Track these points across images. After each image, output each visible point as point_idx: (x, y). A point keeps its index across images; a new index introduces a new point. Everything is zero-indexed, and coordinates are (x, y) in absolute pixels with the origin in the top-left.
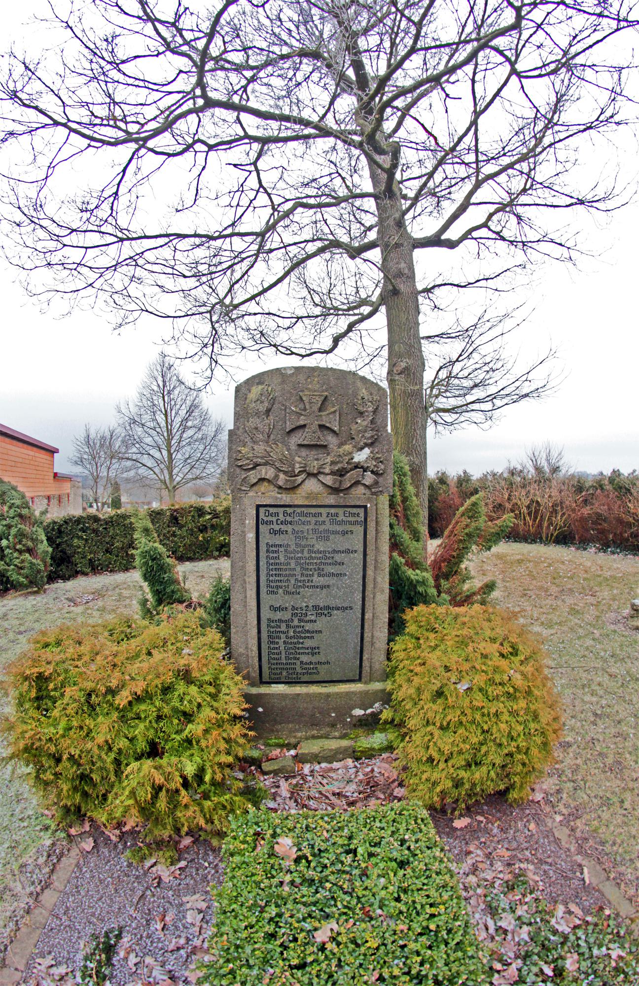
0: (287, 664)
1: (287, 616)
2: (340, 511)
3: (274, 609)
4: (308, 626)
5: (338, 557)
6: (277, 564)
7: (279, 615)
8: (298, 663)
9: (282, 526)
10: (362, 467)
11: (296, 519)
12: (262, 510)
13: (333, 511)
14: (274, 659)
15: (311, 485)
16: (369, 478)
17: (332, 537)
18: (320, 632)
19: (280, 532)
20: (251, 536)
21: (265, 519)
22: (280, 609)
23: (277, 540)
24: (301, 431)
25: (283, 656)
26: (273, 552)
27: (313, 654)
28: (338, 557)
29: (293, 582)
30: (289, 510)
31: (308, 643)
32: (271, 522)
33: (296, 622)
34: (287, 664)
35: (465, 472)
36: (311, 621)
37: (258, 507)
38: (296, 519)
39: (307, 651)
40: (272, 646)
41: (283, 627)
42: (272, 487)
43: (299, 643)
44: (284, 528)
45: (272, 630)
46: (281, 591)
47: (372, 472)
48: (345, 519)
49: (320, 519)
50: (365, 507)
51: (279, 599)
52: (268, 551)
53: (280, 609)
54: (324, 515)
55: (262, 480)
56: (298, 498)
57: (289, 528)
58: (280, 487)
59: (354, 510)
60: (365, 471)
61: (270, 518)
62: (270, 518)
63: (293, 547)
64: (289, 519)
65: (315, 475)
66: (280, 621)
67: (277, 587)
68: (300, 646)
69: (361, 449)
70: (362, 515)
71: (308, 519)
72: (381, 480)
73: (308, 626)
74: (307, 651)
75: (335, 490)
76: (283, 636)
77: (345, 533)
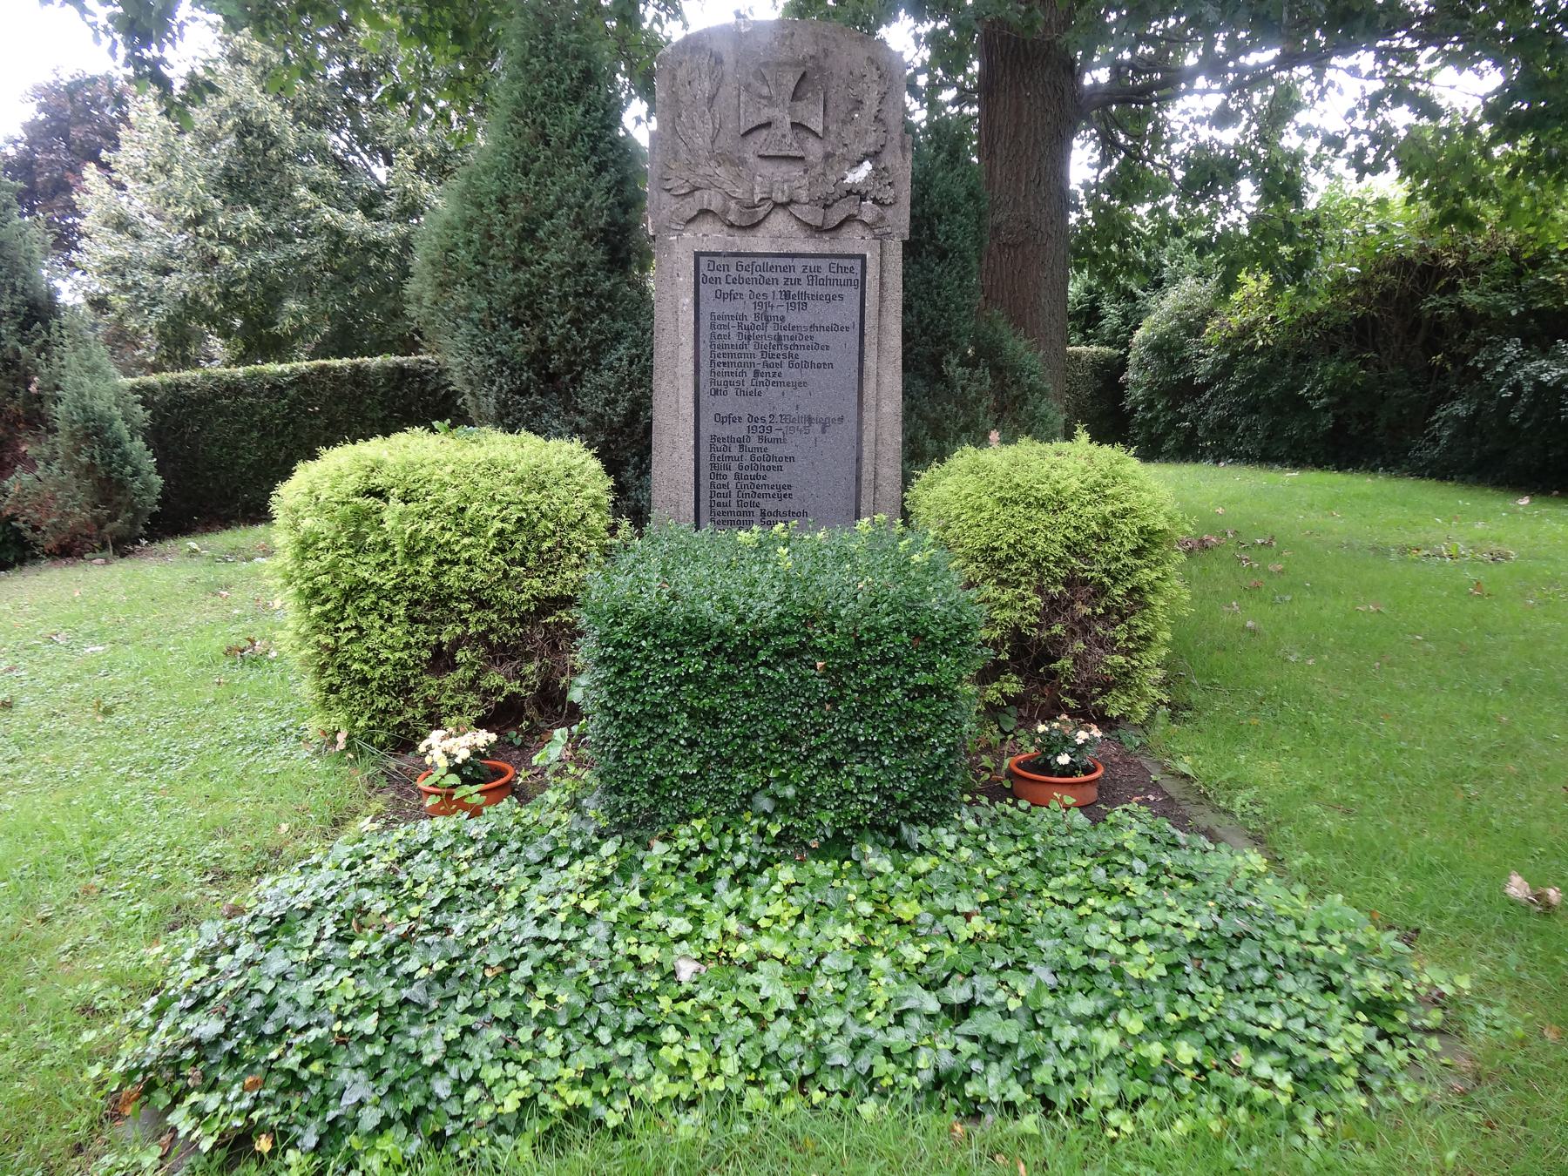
0: (740, 514)
1: (740, 430)
2: (824, 263)
3: (721, 419)
4: (774, 450)
5: (821, 338)
6: (725, 346)
7: (727, 430)
8: (757, 512)
9: (733, 287)
10: (858, 193)
11: (756, 275)
12: (703, 260)
13: (812, 262)
14: (719, 505)
15: (779, 221)
16: (868, 211)
17: (810, 304)
18: (792, 459)
19: (732, 296)
20: (687, 301)
21: (709, 275)
22: (731, 419)
23: (727, 308)
24: (764, 132)
25: (734, 503)
26: (721, 327)
27: (780, 498)
28: (821, 338)
29: (750, 375)
30: (746, 261)
31: (774, 478)
32: (717, 280)
33: (754, 438)
34: (740, 514)
35: (738, 15)
36: (778, 440)
37: (698, 255)
38: (756, 275)
39: (771, 492)
40: (717, 482)
41: (735, 451)
42: (718, 226)
43: (757, 477)
44: (736, 288)
45: (717, 454)
46: (731, 389)
47: (875, 200)
48: (831, 276)
49: (793, 276)
50: (863, 257)
51: (727, 404)
52: (712, 326)
53: (731, 419)
54: (799, 269)
55: (704, 212)
56: (759, 243)
57: (745, 289)
58: (731, 225)
59: (846, 263)
60: (863, 199)
61: (716, 274)
62: (716, 274)
63: (751, 319)
64: (745, 274)
65: (784, 206)
66: (731, 439)
67: (727, 384)
68: (761, 482)
69: (860, 162)
70: (858, 269)
71: (774, 275)
72: (889, 213)
73: (774, 450)
74: (771, 492)
75: (818, 230)
76: (735, 465)
77: (830, 299)
